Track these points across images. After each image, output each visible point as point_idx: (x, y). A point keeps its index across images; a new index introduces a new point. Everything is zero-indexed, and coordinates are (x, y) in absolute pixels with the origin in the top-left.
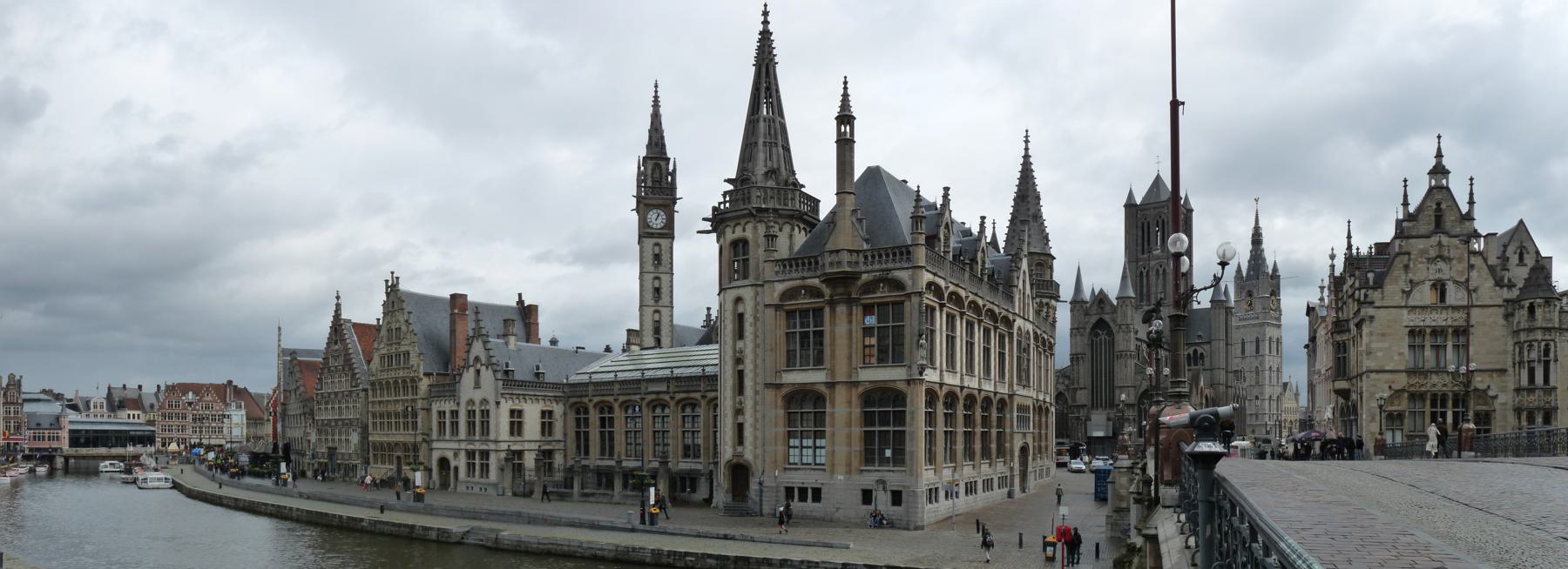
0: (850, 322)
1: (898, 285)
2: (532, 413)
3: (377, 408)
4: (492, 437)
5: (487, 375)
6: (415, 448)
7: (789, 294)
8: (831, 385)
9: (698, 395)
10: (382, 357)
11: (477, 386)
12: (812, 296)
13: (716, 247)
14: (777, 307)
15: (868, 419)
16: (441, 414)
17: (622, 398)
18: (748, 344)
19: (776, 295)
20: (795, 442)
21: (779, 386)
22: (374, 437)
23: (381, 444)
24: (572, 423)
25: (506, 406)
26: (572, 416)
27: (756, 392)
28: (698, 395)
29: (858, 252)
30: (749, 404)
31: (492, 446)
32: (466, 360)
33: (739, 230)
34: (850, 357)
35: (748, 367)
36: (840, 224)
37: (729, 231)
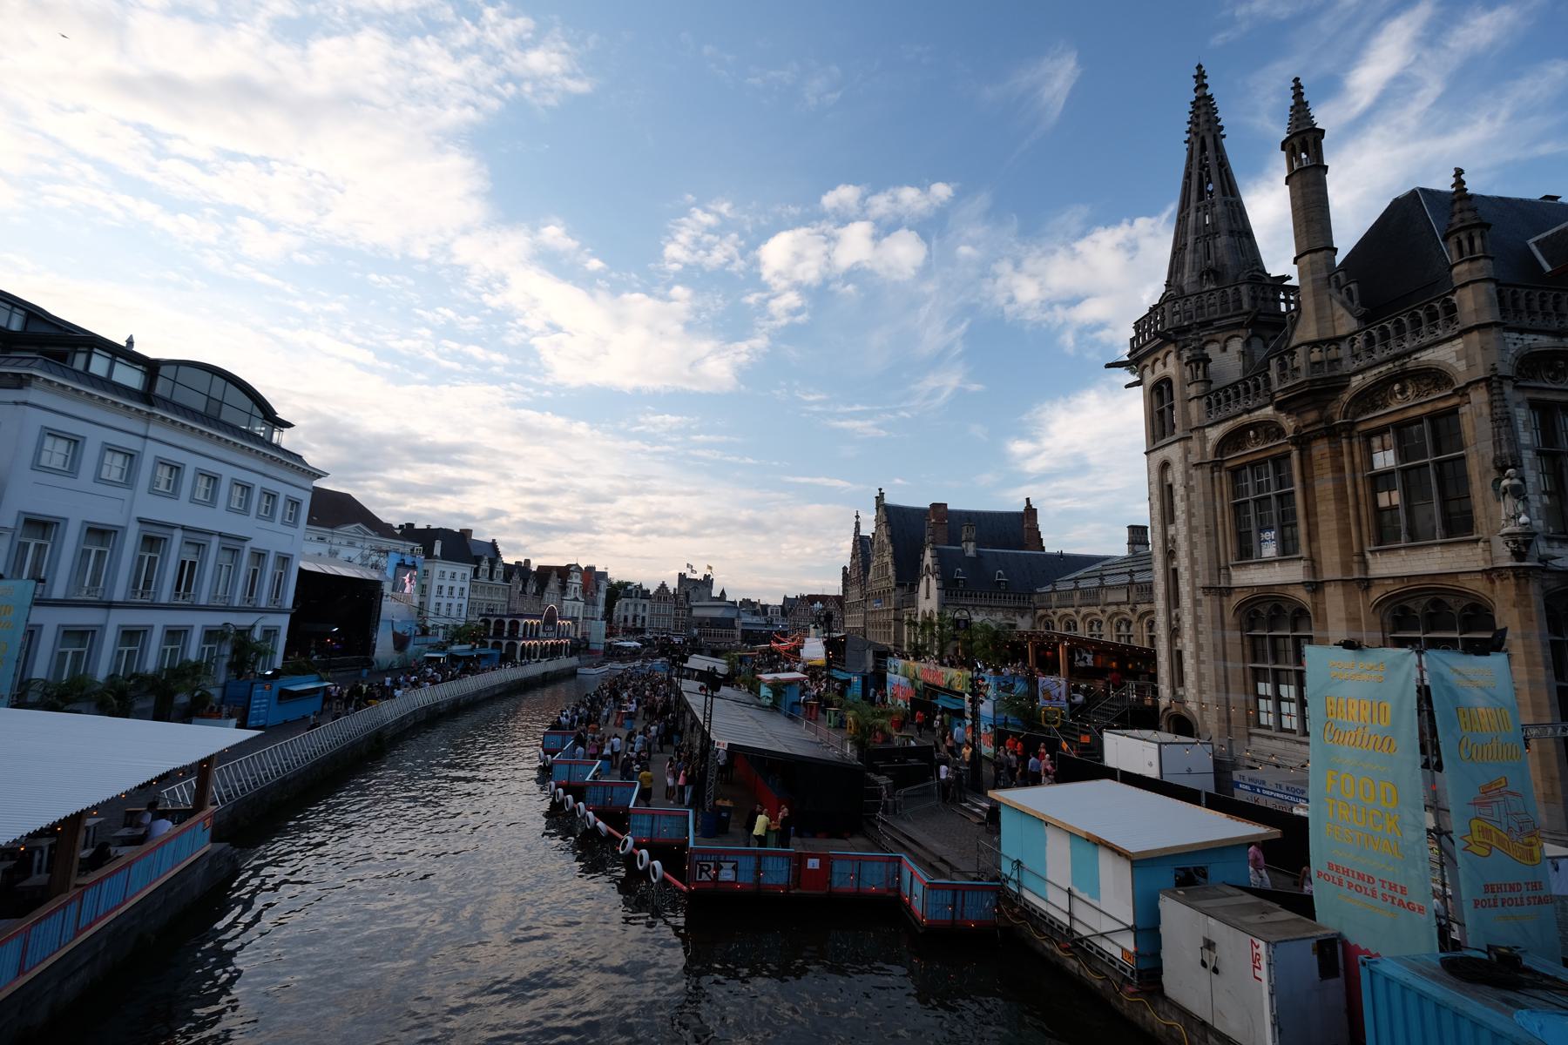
1: (1436, 377)
5: (933, 583)
7: (1233, 440)
8: (1315, 587)
12: (1268, 438)
14: (1216, 465)
17: (1084, 610)
18: (1179, 529)
19: (1209, 447)
20: (1265, 688)
27: (1196, 603)
33: (1159, 365)
34: (1344, 533)
35: (1182, 562)
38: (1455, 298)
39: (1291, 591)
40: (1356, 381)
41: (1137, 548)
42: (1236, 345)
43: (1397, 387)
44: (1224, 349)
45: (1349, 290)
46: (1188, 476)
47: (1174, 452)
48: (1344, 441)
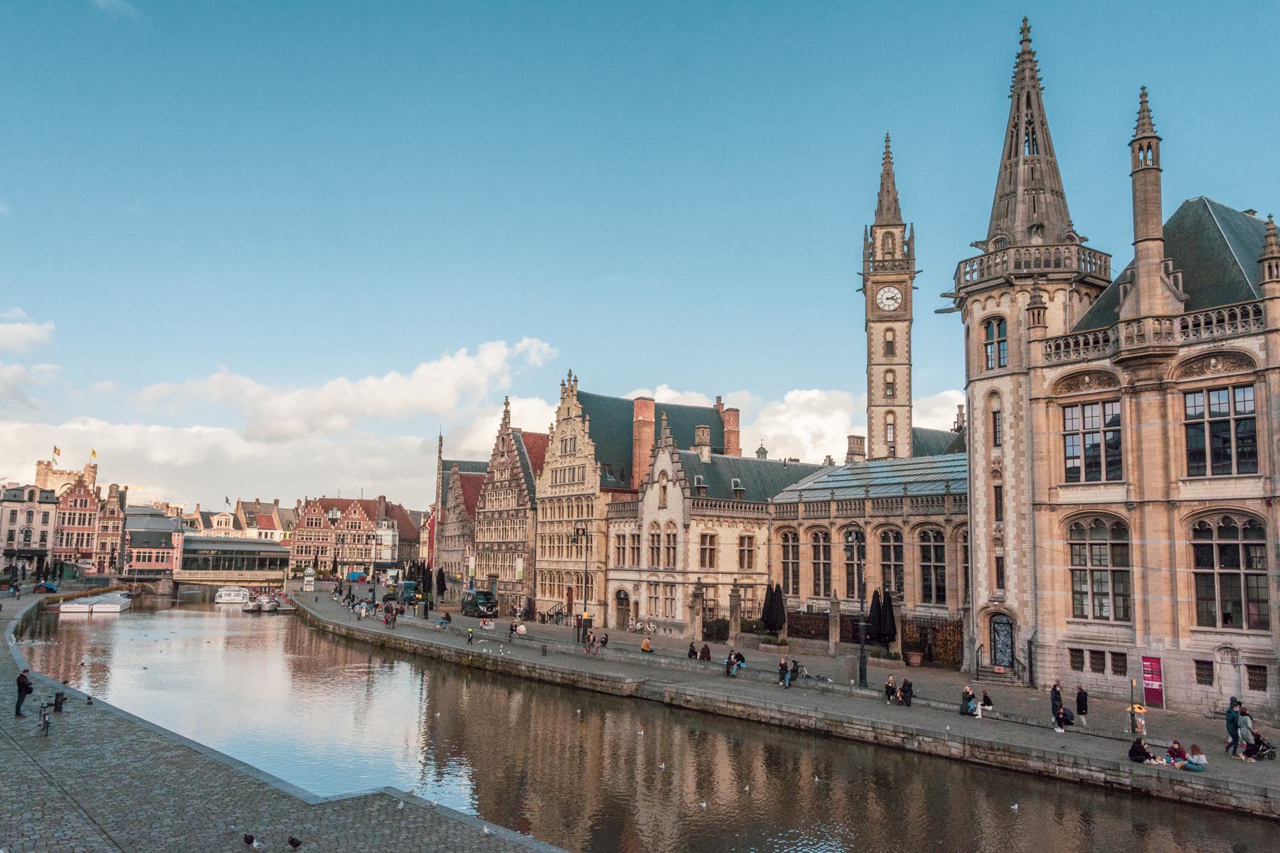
0: (1164, 416)
1: (1242, 359)
2: (728, 536)
3: (547, 530)
4: (679, 567)
5: (675, 493)
6: (587, 578)
9: (941, 519)
10: (554, 471)
11: (663, 506)
13: (963, 328)
14: (1049, 400)
15: (1202, 556)
16: (621, 537)
19: (1046, 385)
21: (1053, 507)
22: (542, 564)
23: (550, 572)
24: (777, 552)
25: (697, 529)
26: (777, 540)
28: (941, 519)
29: (1170, 318)
30: (1011, 532)
31: (679, 578)
32: (651, 475)
35: (1009, 481)
36: (1143, 281)
37: (976, 308)
38: (1261, 306)
39: (1113, 509)
40: (1183, 353)
41: (857, 458)
42: (1060, 297)
43: (1213, 361)
44: (1052, 299)
45: (1176, 280)
46: (1017, 406)
47: (1005, 385)
48: (1169, 396)
